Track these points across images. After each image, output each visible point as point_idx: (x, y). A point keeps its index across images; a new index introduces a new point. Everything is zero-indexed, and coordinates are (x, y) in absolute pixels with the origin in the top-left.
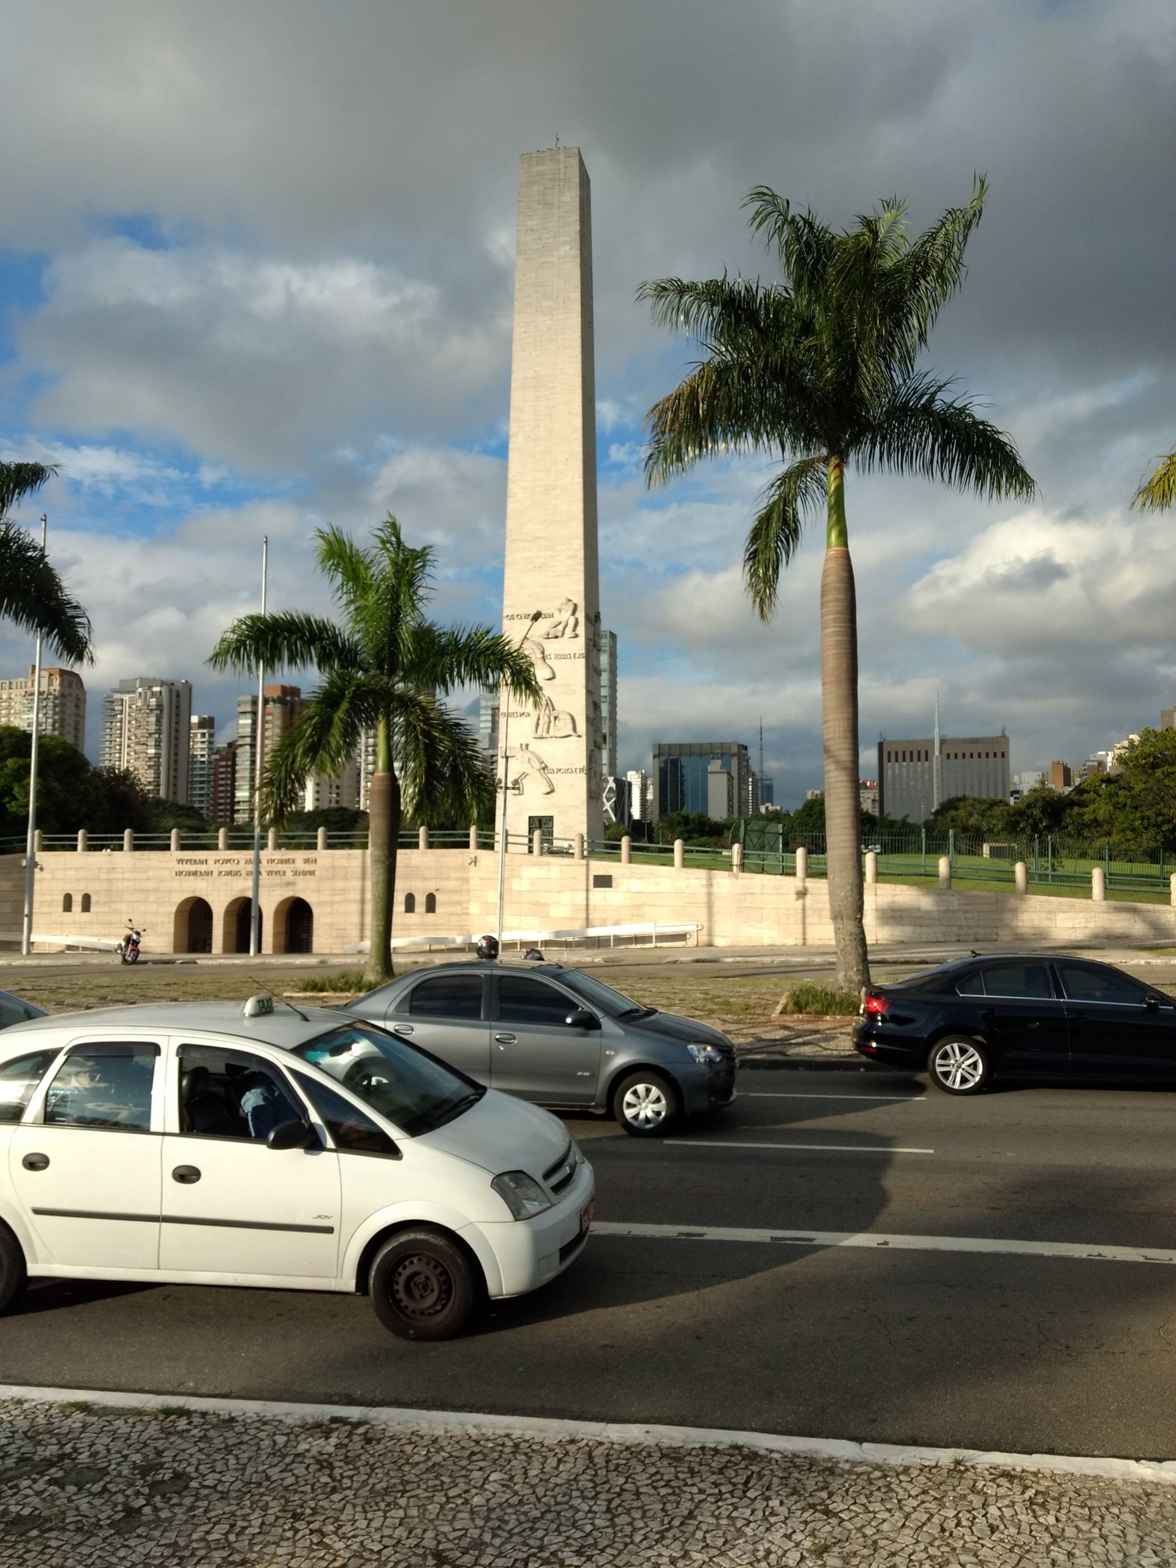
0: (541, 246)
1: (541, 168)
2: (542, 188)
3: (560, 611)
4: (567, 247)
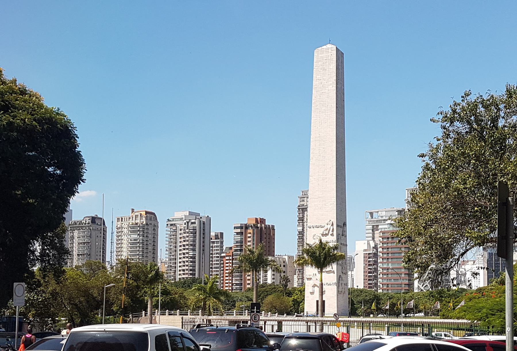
0: (322, 86)
1: (322, 55)
2: (322, 63)
3: (327, 224)
4: (331, 86)
